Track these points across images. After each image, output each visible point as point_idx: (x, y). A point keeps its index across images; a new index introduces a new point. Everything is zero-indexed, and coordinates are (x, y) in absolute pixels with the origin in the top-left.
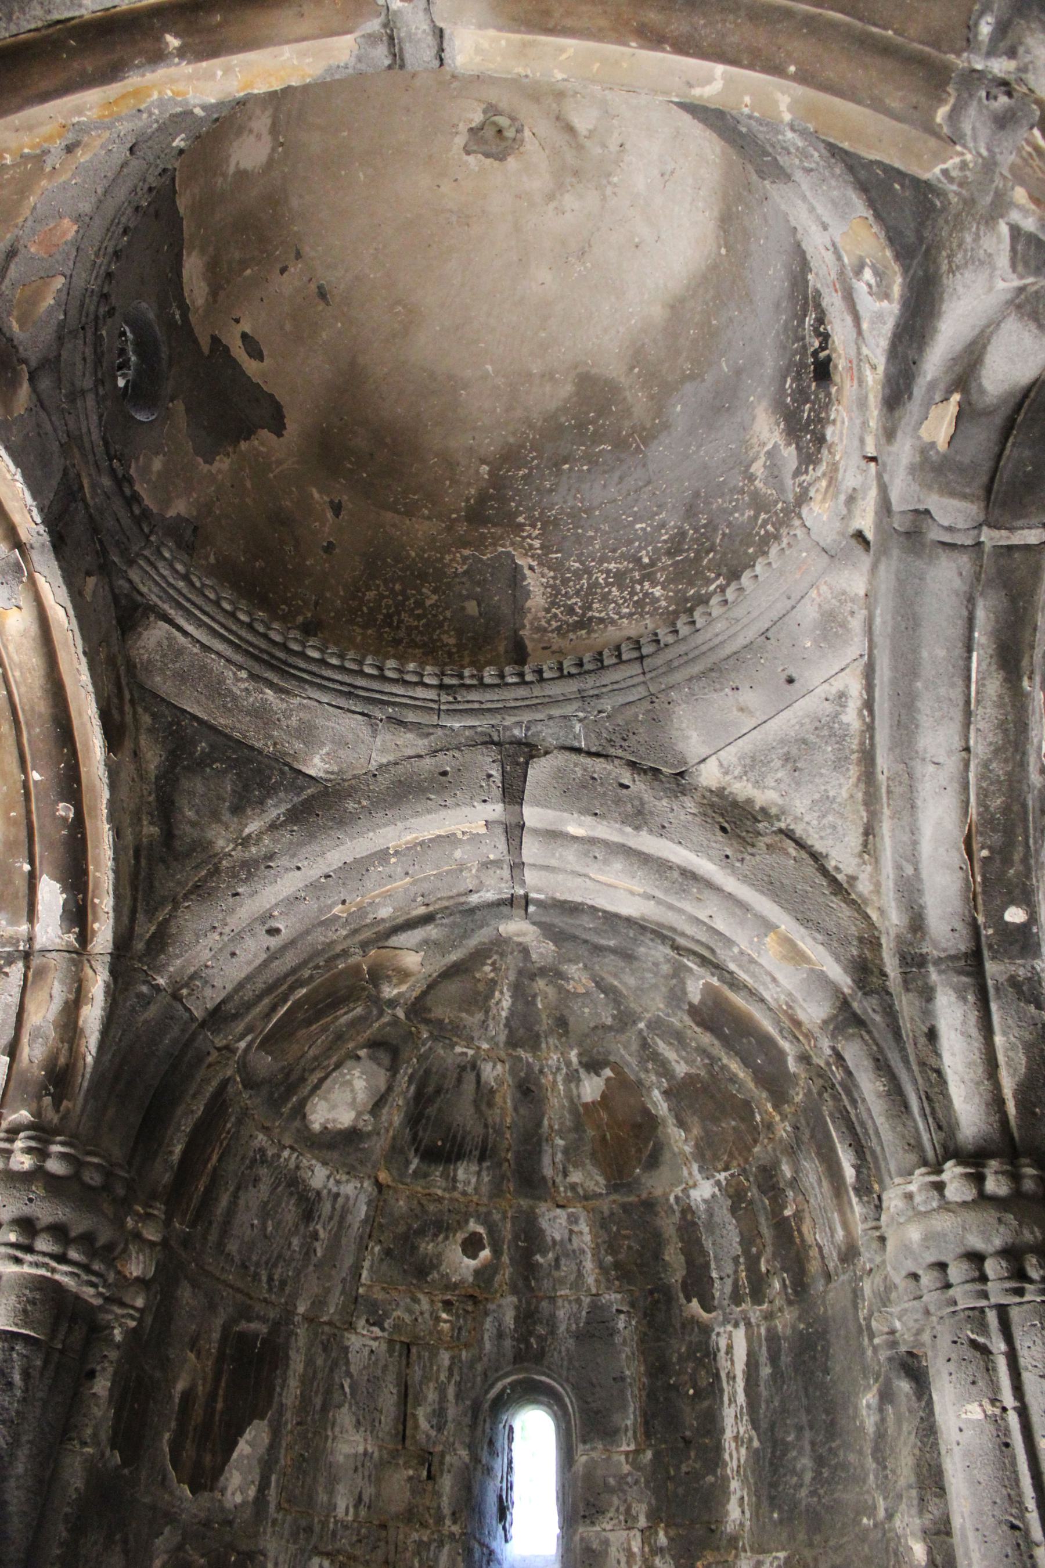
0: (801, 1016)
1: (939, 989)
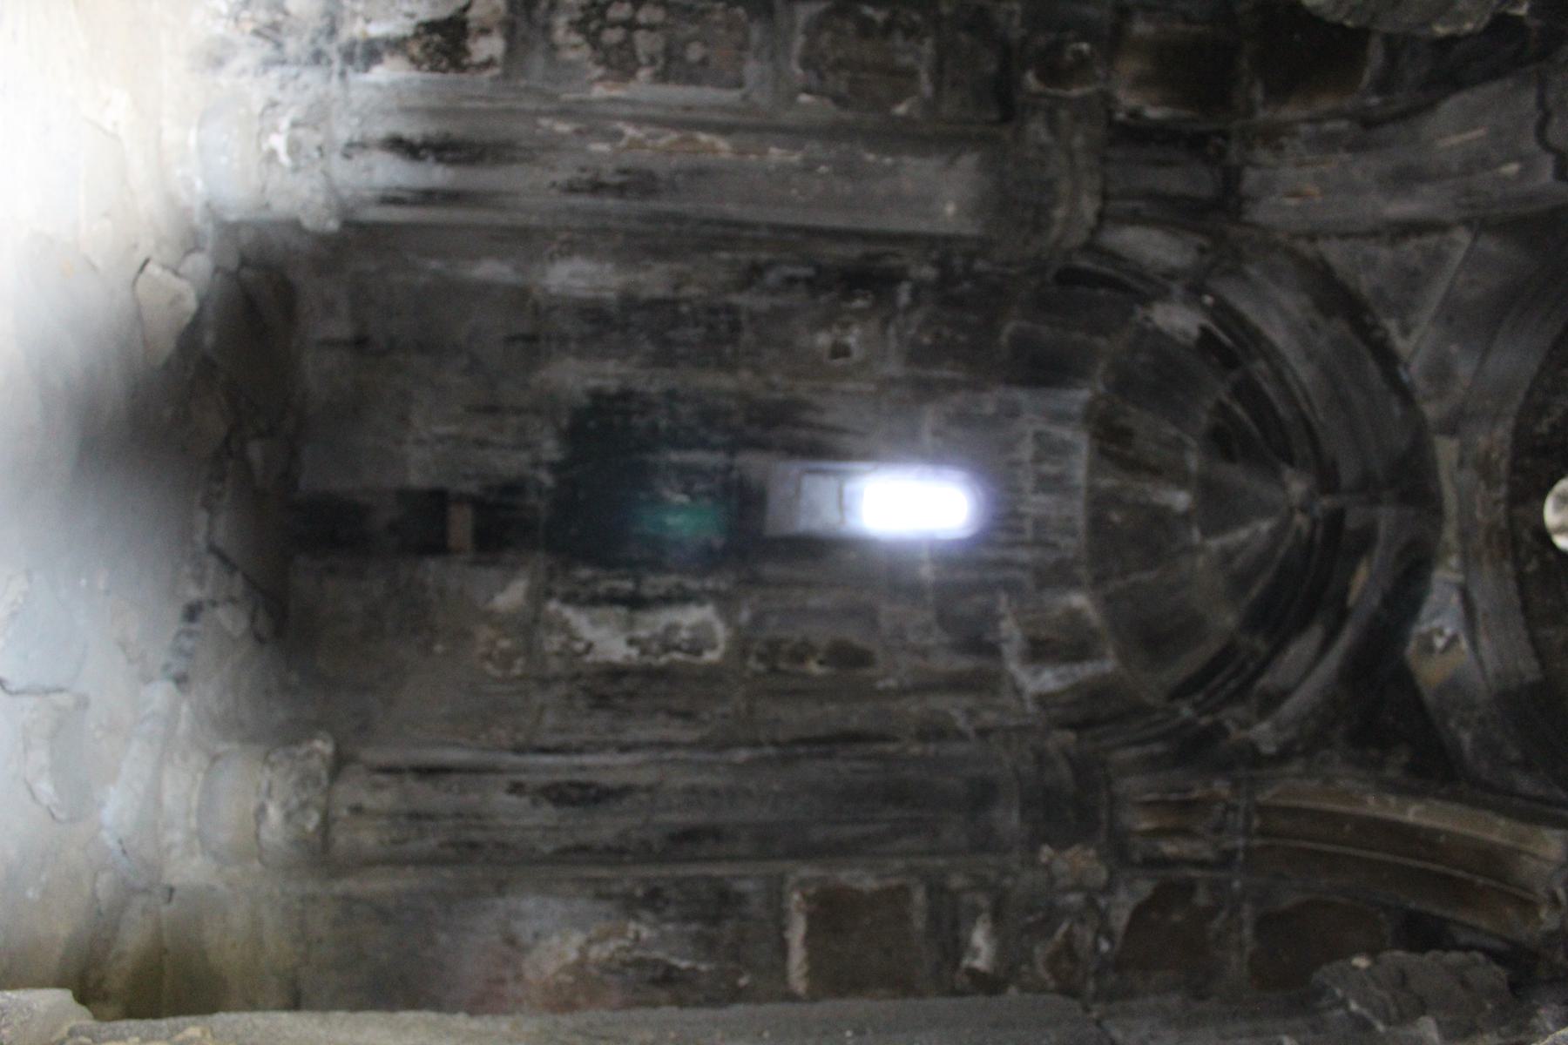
0: (1263, 155)
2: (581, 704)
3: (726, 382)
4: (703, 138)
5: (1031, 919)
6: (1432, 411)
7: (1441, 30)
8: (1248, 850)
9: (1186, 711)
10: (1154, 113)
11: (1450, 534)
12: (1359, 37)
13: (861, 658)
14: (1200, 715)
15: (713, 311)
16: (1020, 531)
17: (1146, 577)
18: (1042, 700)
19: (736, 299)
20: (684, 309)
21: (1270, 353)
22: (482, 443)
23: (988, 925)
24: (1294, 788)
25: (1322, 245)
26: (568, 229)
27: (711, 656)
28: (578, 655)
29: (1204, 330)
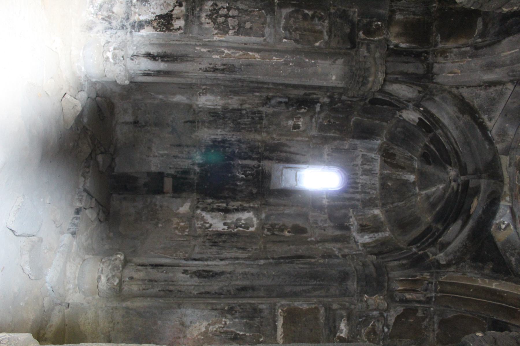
0: (440, 59)
1: (418, 94)
2: (207, 244)
3: (258, 137)
4: (251, 53)
5: (361, 320)
6: (499, 147)
7: (505, 10)
8: (436, 297)
9: (414, 250)
10: (402, 45)
11: (506, 189)
12: (476, 13)
13: (303, 231)
14: (420, 251)
15: (254, 113)
16: (357, 188)
17: (400, 204)
18: (364, 245)
19: (260, 109)
20: (244, 112)
21: (443, 127)
22: (175, 157)
23: (346, 321)
24: (451, 276)
25: (461, 90)
26: (206, 85)
27: (252, 229)
28: (207, 228)
29: (420, 119)
